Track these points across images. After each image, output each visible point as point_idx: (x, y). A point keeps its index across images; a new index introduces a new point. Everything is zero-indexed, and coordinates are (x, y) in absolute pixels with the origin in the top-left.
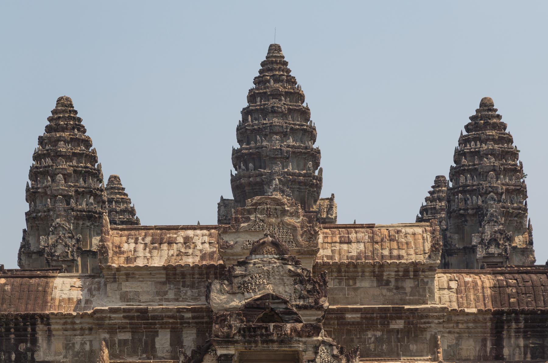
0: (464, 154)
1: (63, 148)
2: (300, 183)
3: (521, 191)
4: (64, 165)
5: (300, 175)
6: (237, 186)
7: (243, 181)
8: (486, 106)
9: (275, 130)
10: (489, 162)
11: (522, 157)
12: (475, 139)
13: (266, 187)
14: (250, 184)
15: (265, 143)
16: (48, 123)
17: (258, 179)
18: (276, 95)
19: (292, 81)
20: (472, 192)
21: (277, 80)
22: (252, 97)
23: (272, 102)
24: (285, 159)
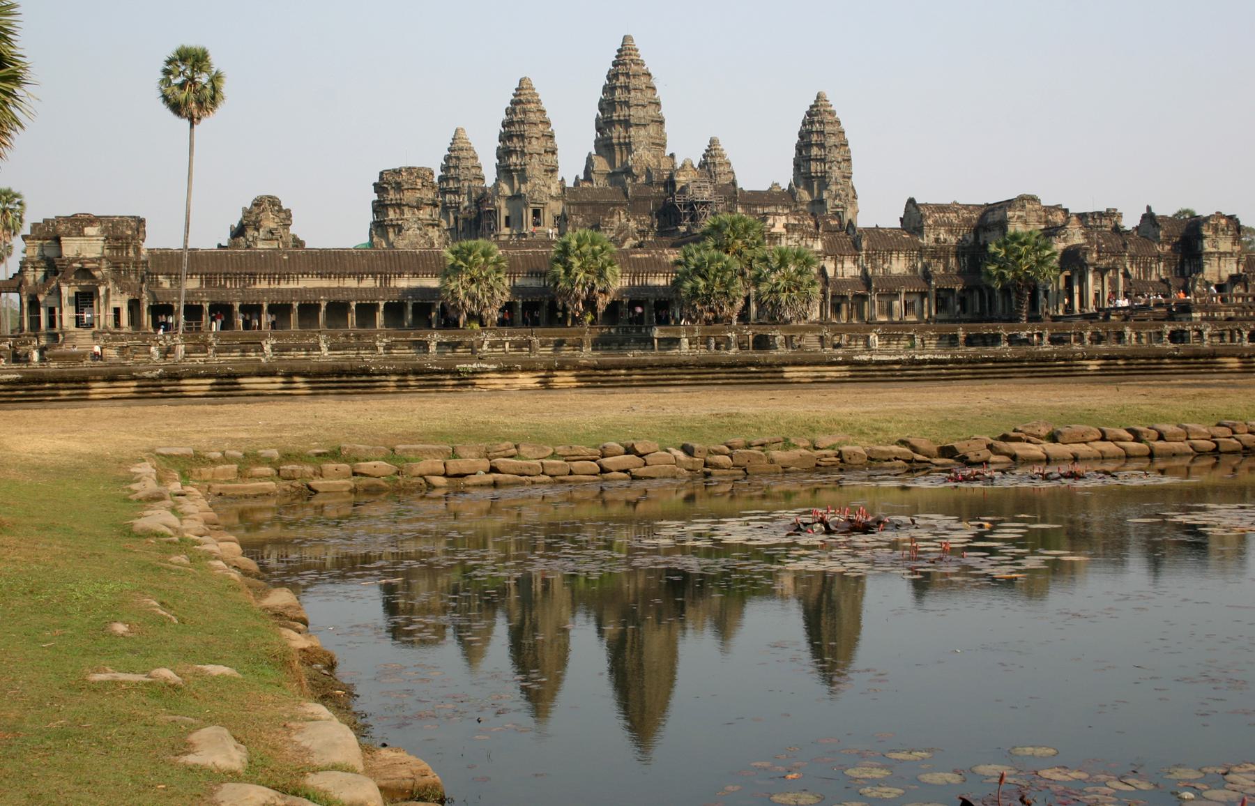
0: (812, 132)
1: (533, 117)
3: (849, 160)
4: (535, 129)
6: (606, 146)
7: (615, 141)
10: (831, 141)
12: (821, 122)
14: (620, 144)
22: (612, 76)
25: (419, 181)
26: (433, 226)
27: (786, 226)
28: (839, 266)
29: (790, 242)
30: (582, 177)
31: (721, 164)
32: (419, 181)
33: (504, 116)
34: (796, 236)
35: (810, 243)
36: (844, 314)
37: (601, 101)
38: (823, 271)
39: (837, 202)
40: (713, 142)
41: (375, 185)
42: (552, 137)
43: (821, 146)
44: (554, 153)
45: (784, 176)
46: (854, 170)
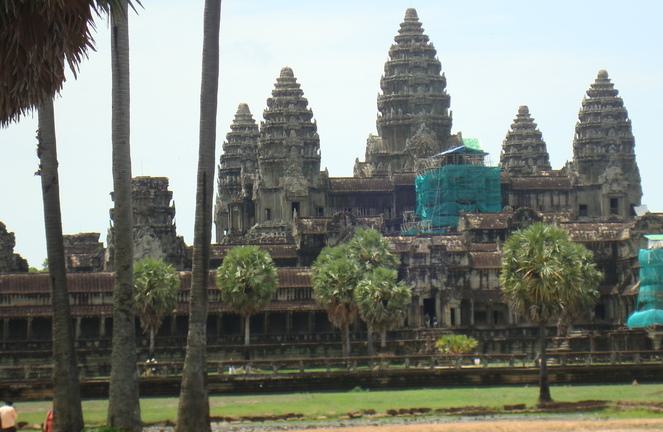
2: (438, 125)
5: (437, 119)
8: (603, 77)
9: (414, 81)
10: (610, 121)
11: (630, 116)
12: (598, 103)
13: (412, 129)
15: (411, 93)
16: (274, 88)
17: (407, 122)
18: (417, 53)
19: (426, 39)
20: (597, 144)
21: (417, 40)
22: (394, 53)
23: (413, 59)
24: (428, 107)
25: (152, 191)
26: (167, 232)
27: (429, 247)
28: (484, 279)
29: (434, 261)
30: (363, 159)
31: (528, 136)
32: (152, 191)
33: (265, 107)
34: (438, 255)
35: (457, 259)
36: (489, 321)
37: (383, 79)
38: (467, 284)
39: (615, 187)
40: (524, 112)
41: (112, 194)
42: (313, 128)
43: (596, 128)
44: (316, 143)
45: (570, 156)
46: (637, 150)
